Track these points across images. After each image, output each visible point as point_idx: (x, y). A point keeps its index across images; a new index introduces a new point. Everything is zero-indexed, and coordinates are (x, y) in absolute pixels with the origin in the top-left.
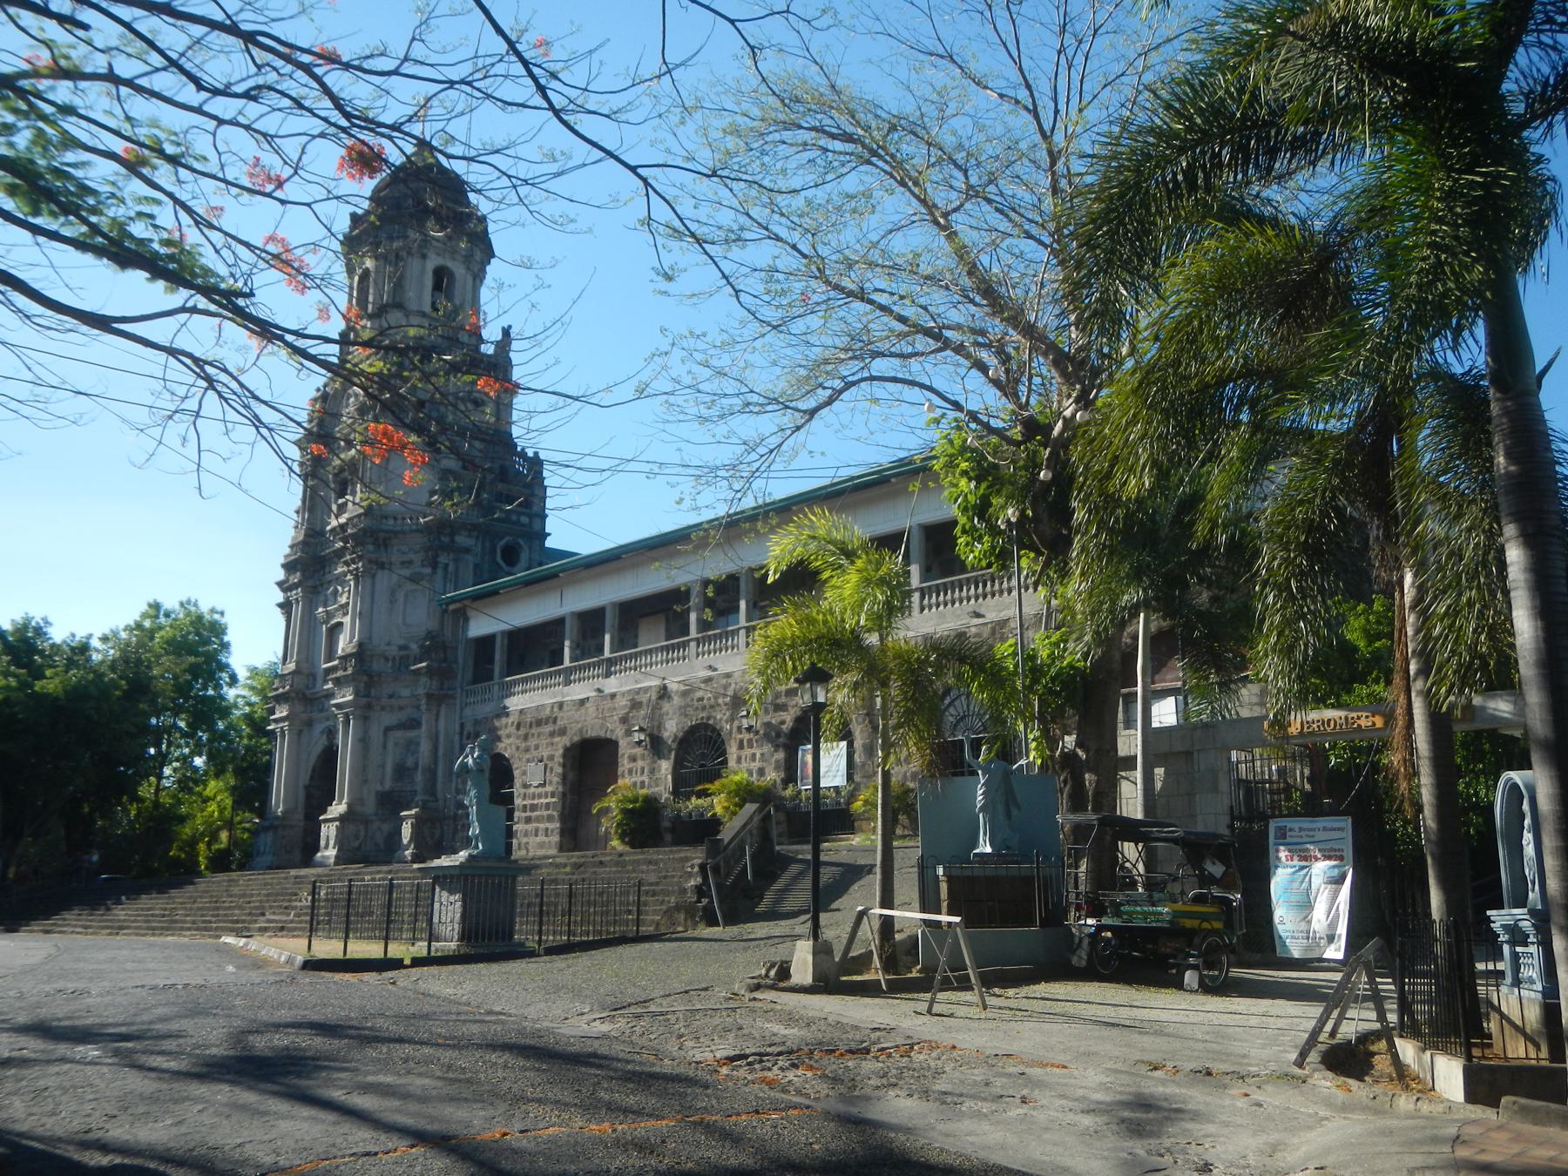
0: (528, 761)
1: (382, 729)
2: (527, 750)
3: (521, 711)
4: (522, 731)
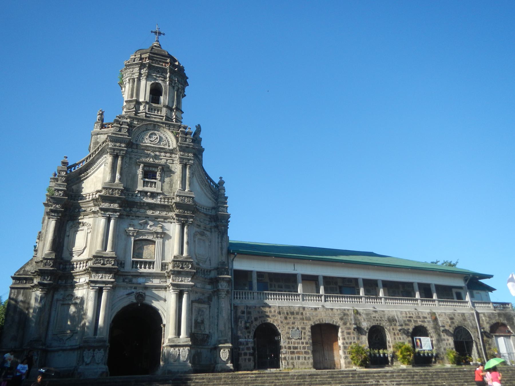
1: (190, 301)
2: (288, 324)
3: (279, 307)
4: (282, 315)
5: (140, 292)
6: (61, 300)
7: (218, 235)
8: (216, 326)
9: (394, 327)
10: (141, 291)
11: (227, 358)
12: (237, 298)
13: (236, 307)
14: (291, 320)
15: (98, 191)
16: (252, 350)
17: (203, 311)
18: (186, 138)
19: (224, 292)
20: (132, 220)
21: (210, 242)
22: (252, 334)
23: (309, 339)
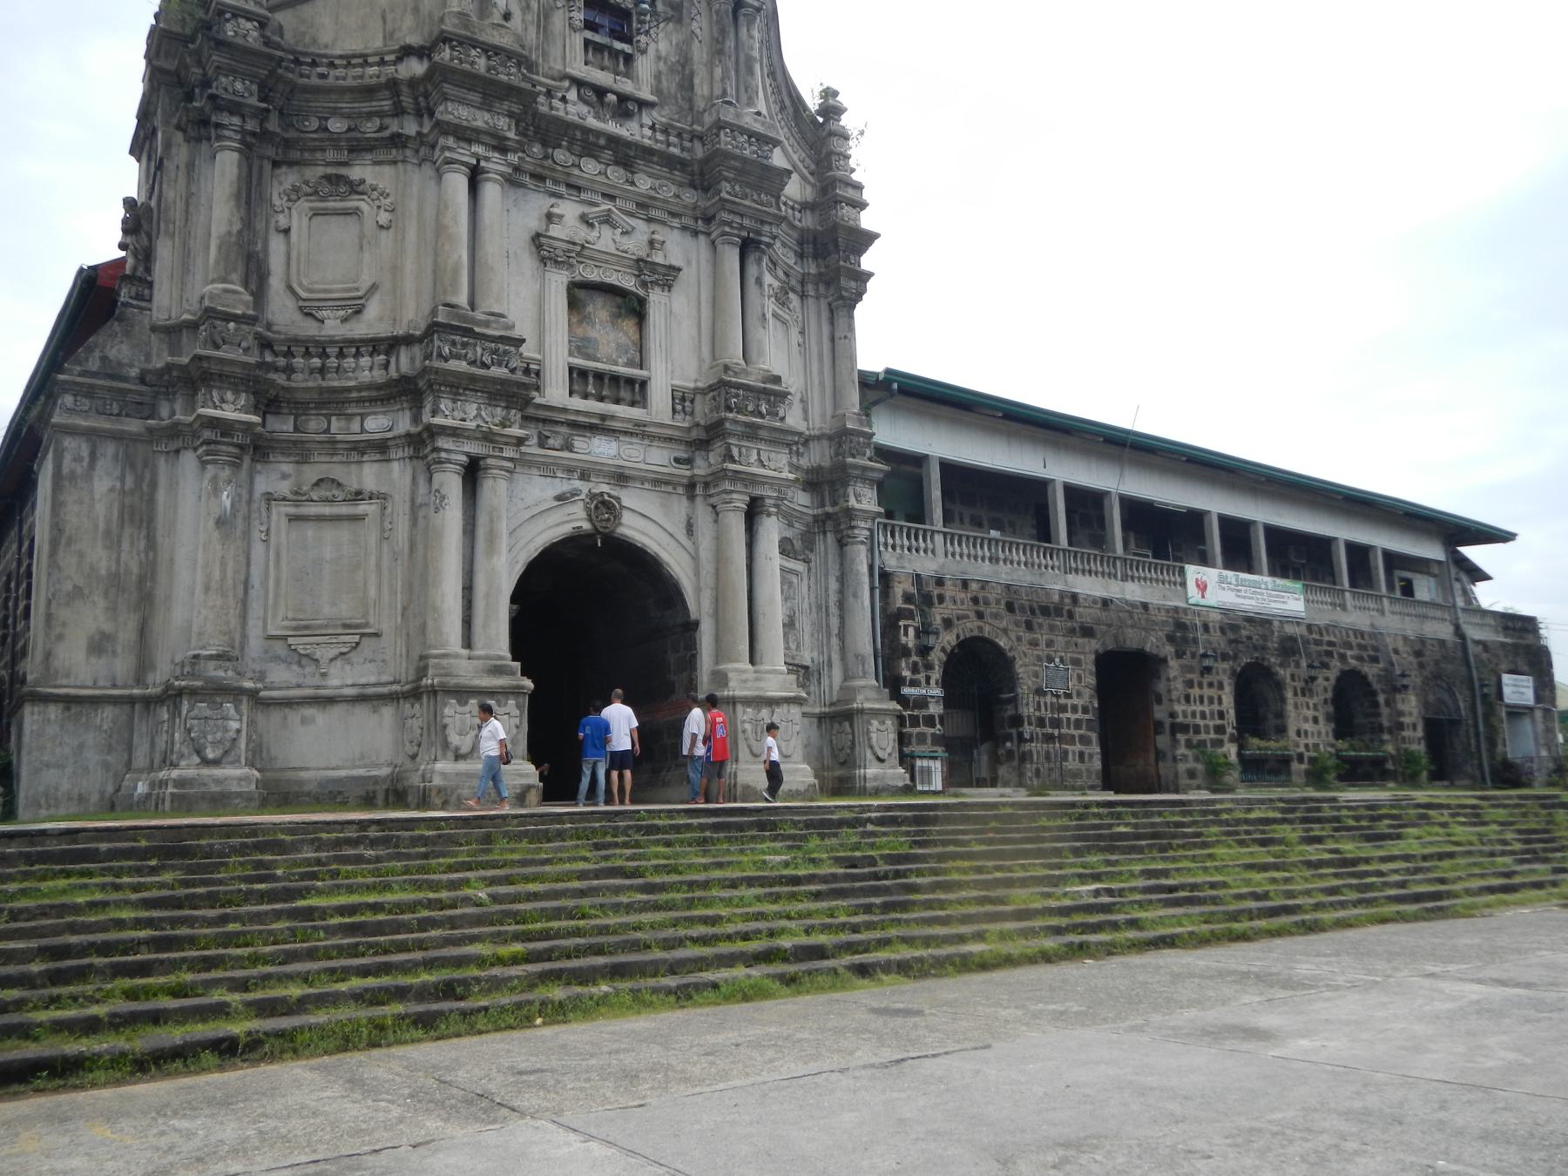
2: (1034, 644)
3: (1008, 587)
5: (602, 494)
6: (284, 499)
7: (832, 311)
8: (835, 641)
9: (1296, 671)
10: (605, 488)
11: (889, 750)
12: (886, 545)
13: (886, 578)
14: (1042, 638)
15: (406, 52)
16: (938, 726)
17: (791, 584)
19: (865, 520)
20: (553, 200)
21: (802, 333)
22: (936, 675)
23: (1091, 697)
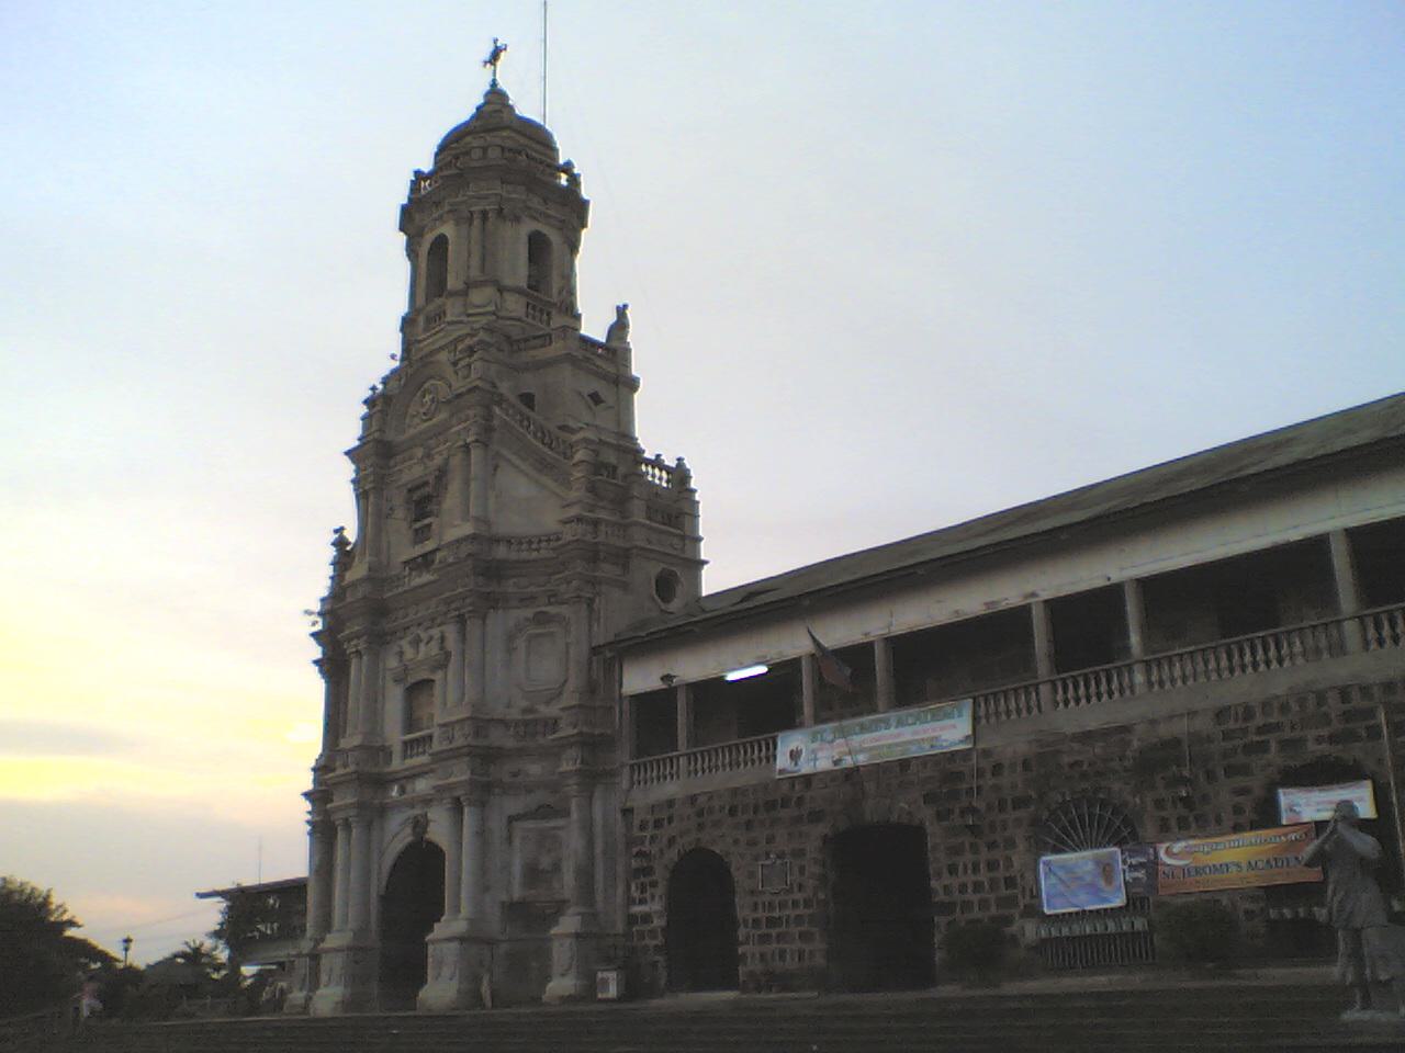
0: (756, 859)
1: (504, 820)
2: (752, 843)
3: (735, 792)
10: (417, 811)
16: (660, 938)
18: (469, 365)
22: (660, 890)
